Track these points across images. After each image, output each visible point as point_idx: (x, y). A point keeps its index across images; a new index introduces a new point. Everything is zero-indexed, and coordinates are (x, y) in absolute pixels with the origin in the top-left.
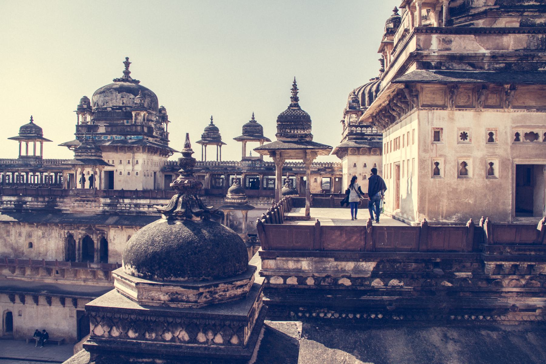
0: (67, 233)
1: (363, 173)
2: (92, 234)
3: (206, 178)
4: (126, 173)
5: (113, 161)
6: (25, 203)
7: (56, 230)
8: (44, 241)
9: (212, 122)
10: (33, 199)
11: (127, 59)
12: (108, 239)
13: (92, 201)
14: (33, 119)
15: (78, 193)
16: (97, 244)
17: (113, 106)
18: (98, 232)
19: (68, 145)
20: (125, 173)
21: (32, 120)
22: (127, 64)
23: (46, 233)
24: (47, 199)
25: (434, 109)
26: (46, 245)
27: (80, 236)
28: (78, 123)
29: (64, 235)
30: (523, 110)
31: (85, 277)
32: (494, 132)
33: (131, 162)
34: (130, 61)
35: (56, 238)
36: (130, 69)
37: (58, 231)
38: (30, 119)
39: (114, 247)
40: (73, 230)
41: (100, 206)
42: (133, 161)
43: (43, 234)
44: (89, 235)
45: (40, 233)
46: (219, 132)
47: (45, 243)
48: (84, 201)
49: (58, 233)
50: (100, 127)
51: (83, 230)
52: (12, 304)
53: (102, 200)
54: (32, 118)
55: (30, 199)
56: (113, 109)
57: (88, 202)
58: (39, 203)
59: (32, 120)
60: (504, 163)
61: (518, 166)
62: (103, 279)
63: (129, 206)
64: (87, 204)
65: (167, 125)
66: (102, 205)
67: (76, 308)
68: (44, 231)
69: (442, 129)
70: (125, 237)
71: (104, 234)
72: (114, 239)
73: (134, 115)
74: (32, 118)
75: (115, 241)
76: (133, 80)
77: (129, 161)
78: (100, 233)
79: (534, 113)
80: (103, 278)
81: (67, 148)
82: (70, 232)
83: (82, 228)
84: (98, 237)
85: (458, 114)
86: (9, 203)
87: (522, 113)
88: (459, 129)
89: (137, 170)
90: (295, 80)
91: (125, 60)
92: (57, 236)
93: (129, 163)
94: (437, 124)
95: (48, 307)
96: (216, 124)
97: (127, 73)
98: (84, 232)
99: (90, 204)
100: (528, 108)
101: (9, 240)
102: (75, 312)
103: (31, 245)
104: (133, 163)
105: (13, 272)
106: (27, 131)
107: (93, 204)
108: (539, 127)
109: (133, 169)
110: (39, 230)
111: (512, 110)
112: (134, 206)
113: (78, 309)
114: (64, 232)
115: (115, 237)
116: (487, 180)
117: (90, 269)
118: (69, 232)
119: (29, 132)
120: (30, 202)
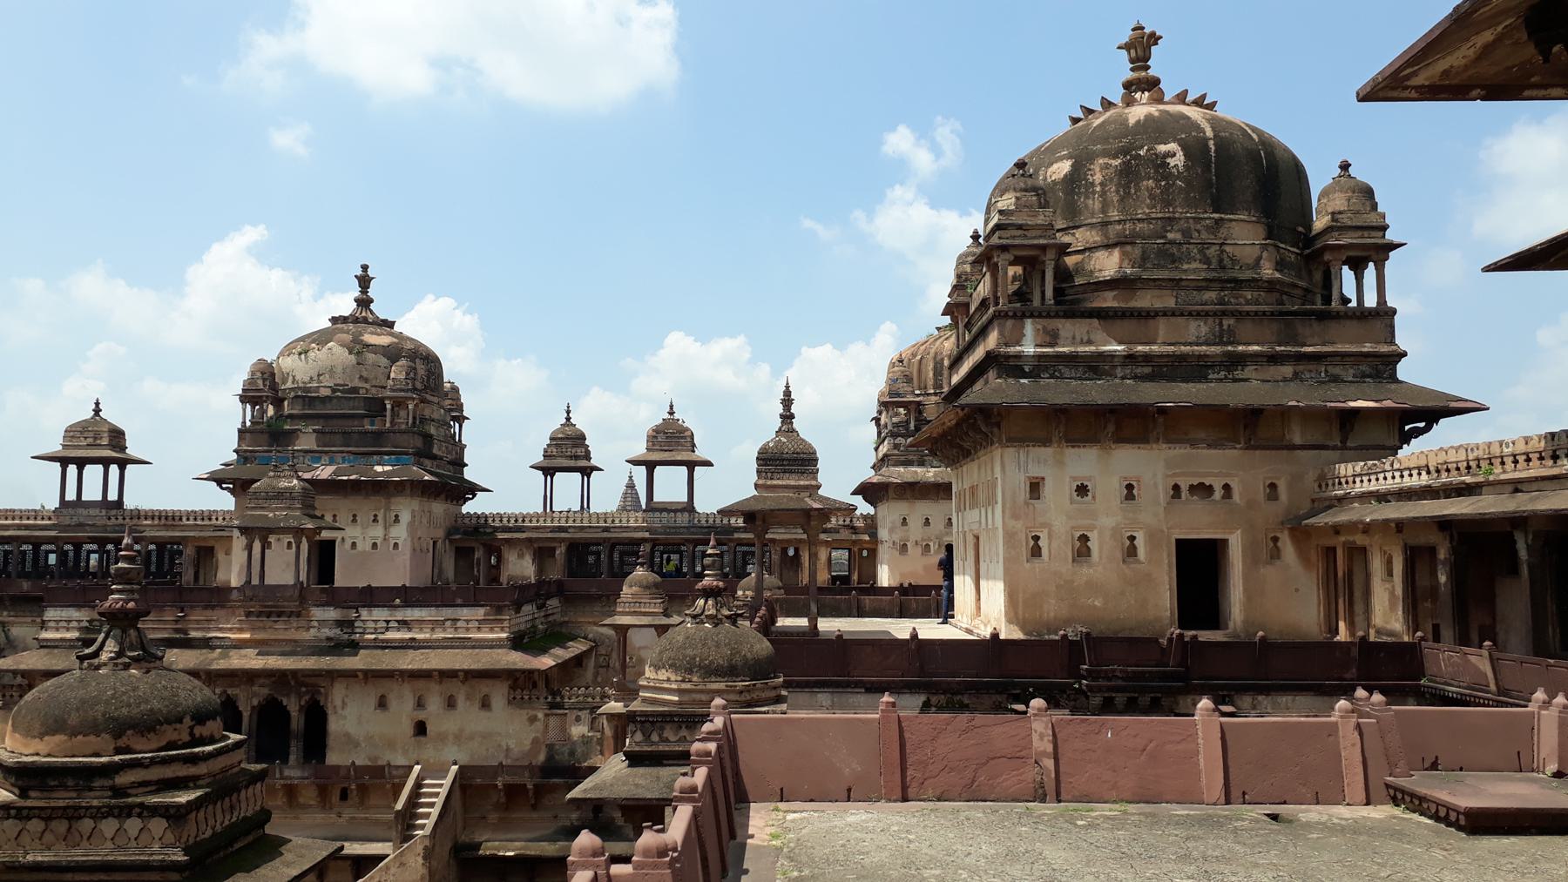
1: (923, 540)
2: (288, 695)
3: (557, 552)
4: (368, 547)
5: (335, 516)
9: (568, 419)
11: (365, 268)
12: (329, 704)
13: (291, 614)
14: (101, 407)
15: (253, 596)
16: (297, 721)
17: (335, 385)
18: (304, 689)
19: (218, 479)
20: (364, 546)
21: (97, 411)
22: (364, 281)
25: (1028, 446)
27: (255, 702)
28: (244, 422)
30: (1184, 445)
32: (1134, 483)
33: (380, 518)
34: (371, 273)
36: (371, 293)
38: (94, 406)
39: (344, 725)
40: (238, 686)
41: (308, 629)
42: (385, 516)
44: (279, 699)
46: (587, 442)
48: (269, 615)
50: (301, 435)
53: (318, 613)
54: (97, 404)
56: (334, 391)
57: (279, 616)
59: (97, 411)
60: (1152, 537)
61: (1178, 541)
63: (384, 625)
64: (276, 622)
65: (461, 427)
66: (316, 624)
69: (1043, 479)
70: (373, 701)
71: (319, 693)
72: (344, 704)
73: (388, 407)
74: (97, 404)
75: (345, 712)
76: (382, 320)
77: (375, 516)
78: (307, 692)
79: (1205, 451)
80: (312, 802)
81: (215, 484)
82: (229, 692)
83: (262, 681)
84: (303, 703)
85: (1072, 454)
86: (65, 624)
87: (1182, 451)
88: (1074, 479)
89: (398, 538)
90: (788, 383)
91: (359, 272)
93: (375, 520)
94: (1035, 472)
96: (579, 421)
97: (364, 302)
98: (265, 691)
100: (1193, 444)
104: (385, 521)
106: (86, 438)
107: (294, 622)
108: (1216, 475)
109: (385, 535)
111: (1164, 446)
112: (396, 625)
115: (346, 700)
116: (1124, 567)
117: (282, 782)
118: (225, 692)
119: (90, 440)
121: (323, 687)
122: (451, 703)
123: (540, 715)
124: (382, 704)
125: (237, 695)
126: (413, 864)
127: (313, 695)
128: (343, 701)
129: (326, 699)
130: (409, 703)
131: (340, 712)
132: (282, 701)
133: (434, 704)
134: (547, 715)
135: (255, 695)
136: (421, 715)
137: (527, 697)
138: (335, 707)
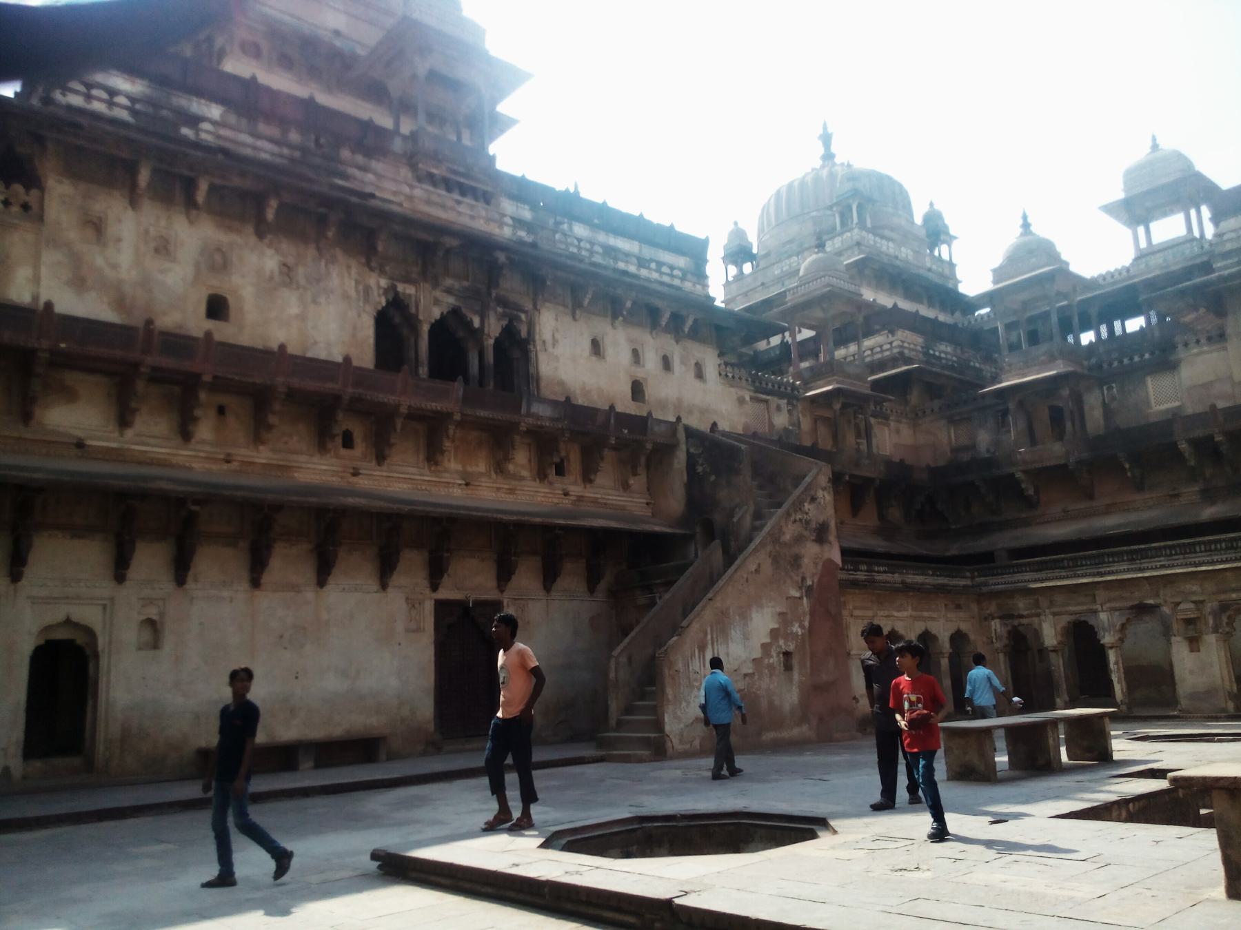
0: (386, 291)
6: (194, 121)
7: (349, 267)
8: (291, 303)
10: (232, 119)
12: (537, 337)
18: (500, 310)
23: (301, 271)
24: (294, 137)
26: (302, 317)
29: (379, 295)
31: (459, 467)
35: (346, 297)
37: (354, 271)
43: (287, 270)
45: (270, 262)
47: (294, 310)
49: (357, 282)
51: (449, 291)
52: (105, 588)
55: (215, 112)
58: (260, 143)
62: (522, 478)
63: (588, 246)
66: (510, 221)
67: (434, 587)
68: (290, 260)
72: (555, 342)
75: (559, 351)
80: (525, 473)
82: (401, 287)
83: (449, 282)
86: (105, 96)
92: (353, 293)
95: (309, 594)
98: (451, 300)
99: (472, 207)
101: (99, 261)
102: (429, 606)
103: (217, 307)
105: (124, 420)
110: (270, 252)
113: (444, 594)
114: (379, 287)
115: (557, 336)
118: (394, 288)
120: (214, 123)
121: (526, 312)
122: (667, 364)
123: (747, 398)
124: (596, 347)
125: (410, 295)
126: (822, 501)
127: (511, 321)
128: (553, 336)
129: (531, 325)
130: (625, 357)
131: (550, 349)
132: (471, 319)
133: (651, 361)
134: (751, 398)
135: (437, 302)
136: (640, 373)
137: (730, 375)
138: (544, 342)
